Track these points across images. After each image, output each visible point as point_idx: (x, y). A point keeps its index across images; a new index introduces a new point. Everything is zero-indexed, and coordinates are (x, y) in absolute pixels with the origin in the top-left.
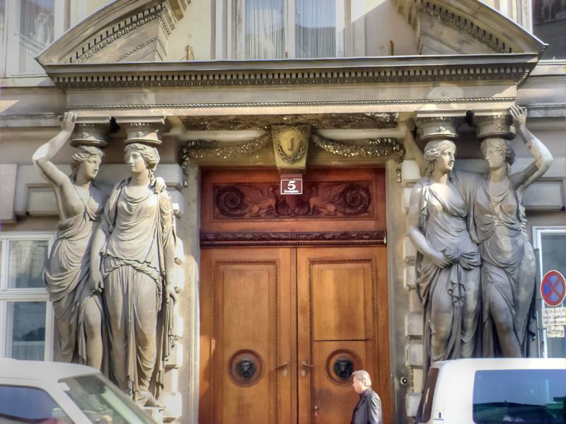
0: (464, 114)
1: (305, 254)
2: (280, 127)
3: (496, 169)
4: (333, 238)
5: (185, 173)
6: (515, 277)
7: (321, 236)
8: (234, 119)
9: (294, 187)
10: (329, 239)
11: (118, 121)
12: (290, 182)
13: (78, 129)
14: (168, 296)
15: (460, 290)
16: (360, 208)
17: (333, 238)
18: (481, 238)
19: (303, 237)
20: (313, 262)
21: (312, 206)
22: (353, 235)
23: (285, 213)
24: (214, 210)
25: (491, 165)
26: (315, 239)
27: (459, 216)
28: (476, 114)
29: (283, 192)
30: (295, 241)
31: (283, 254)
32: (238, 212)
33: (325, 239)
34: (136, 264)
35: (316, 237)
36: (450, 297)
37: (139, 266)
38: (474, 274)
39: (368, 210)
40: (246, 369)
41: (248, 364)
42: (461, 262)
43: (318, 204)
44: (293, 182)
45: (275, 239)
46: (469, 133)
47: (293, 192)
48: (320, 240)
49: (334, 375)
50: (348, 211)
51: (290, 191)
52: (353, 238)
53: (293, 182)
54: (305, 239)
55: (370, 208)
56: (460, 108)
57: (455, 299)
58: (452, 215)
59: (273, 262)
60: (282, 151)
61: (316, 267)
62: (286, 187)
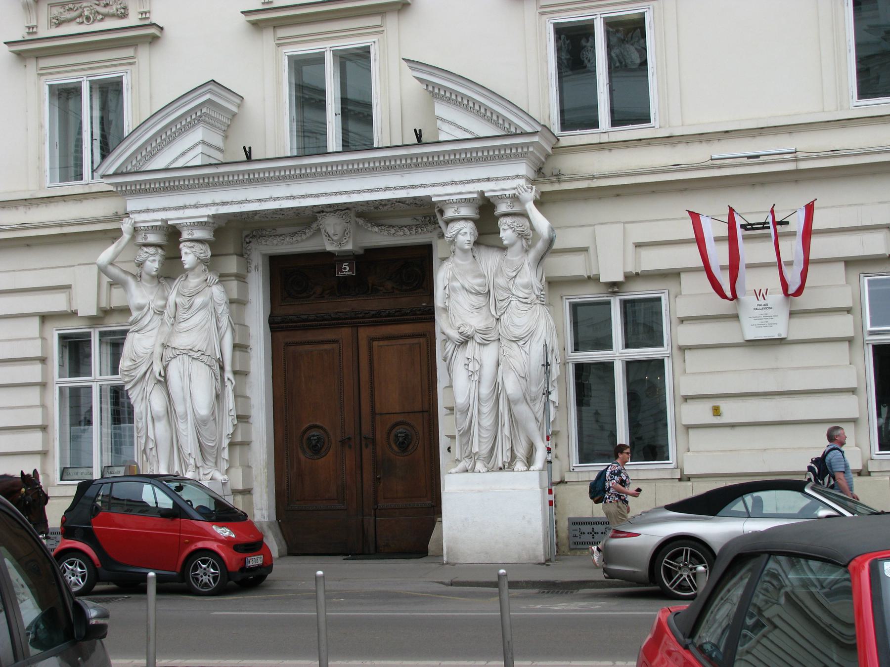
1: (364, 333)
4: (389, 315)
6: (527, 349)
7: (378, 314)
10: (386, 317)
13: (136, 230)
14: (226, 379)
17: (389, 315)
18: (499, 314)
25: (505, 242)
30: (355, 321)
31: (345, 333)
33: (381, 317)
34: (192, 353)
37: (196, 355)
38: (493, 347)
40: (314, 442)
42: (476, 337)
46: (486, 215)
48: (378, 319)
49: (394, 446)
50: (404, 288)
52: (407, 314)
54: (363, 317)
56: (472, 190)
58: (471, 293)
59: (335, 341)
61: (375, 343)
62: (340, 270)
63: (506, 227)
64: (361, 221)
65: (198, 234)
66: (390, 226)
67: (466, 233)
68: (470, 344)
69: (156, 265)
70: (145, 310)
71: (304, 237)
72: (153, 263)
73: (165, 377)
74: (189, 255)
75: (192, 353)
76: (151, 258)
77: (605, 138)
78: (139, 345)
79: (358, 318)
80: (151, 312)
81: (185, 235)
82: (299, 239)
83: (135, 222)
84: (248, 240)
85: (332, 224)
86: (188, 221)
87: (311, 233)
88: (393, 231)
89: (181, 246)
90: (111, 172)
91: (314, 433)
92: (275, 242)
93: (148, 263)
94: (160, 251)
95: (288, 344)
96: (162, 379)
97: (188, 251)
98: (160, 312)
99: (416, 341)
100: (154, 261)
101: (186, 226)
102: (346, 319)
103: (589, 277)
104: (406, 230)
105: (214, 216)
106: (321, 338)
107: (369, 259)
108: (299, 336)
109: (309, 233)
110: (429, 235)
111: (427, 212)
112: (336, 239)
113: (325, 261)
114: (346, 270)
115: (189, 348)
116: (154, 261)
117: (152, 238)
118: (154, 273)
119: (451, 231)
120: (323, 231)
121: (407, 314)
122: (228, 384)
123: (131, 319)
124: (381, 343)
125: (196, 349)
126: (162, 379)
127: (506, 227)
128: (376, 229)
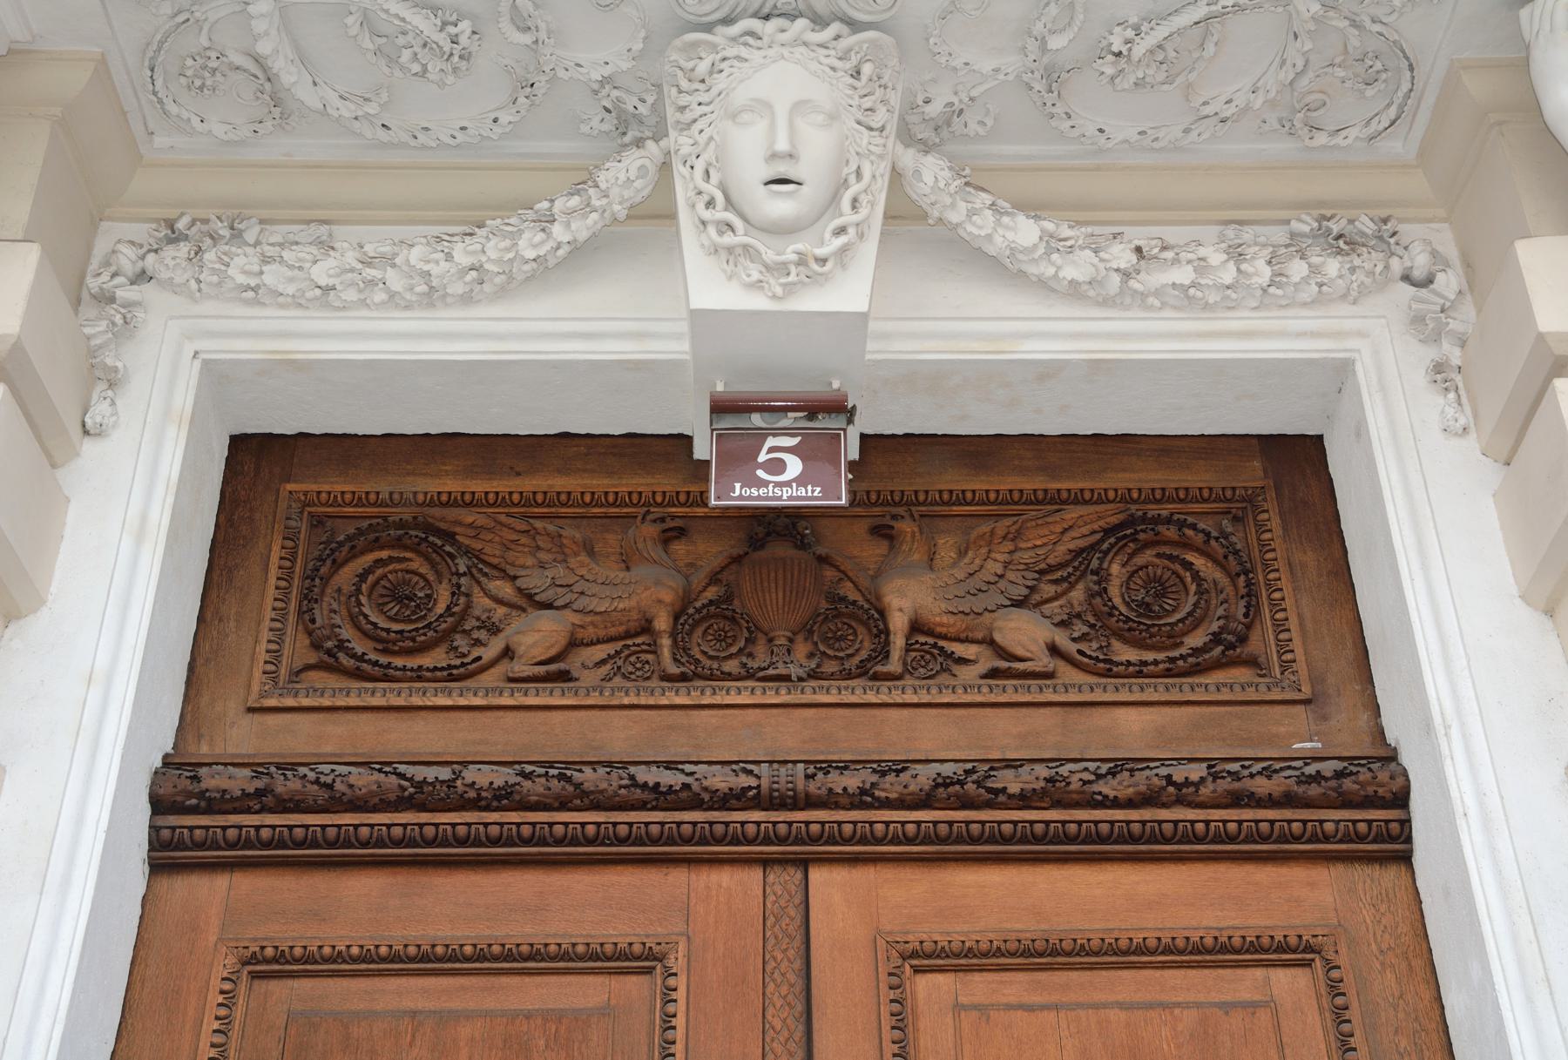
1: (852, 906)
7: (967, 787)
10: (1025, 800)
12: (771, 442)
16: (1196, 639)
17: (1052, 794)
19: (852, 781)
21: (898, 623)
22: (1179, 775)
23: (732, 666)
24: (278, 637)
26: (924, 801)
30: (785, 827)
32: (436, 658)
33: (996, 799)
35: (944, 782)
39: (1254, 645)
43: (935, 610)
45: (660, 797)
47: (786, 493)
50: (1125, 653)
54: (863, 799)
55: (1262, 641)
59: (639, 960)
60: (730, 203)
61: (931, 990)
71: (530, 244)
79: (829, 801)
82: (495, 249)
87: (582, 228)
95: (269, 965)
99: (1245, 983)
102: (727, 800)
106: (521, 931)
108: (362, 906)
110: (1342, 317)
121: (1183, 794)
124: (980, 987)
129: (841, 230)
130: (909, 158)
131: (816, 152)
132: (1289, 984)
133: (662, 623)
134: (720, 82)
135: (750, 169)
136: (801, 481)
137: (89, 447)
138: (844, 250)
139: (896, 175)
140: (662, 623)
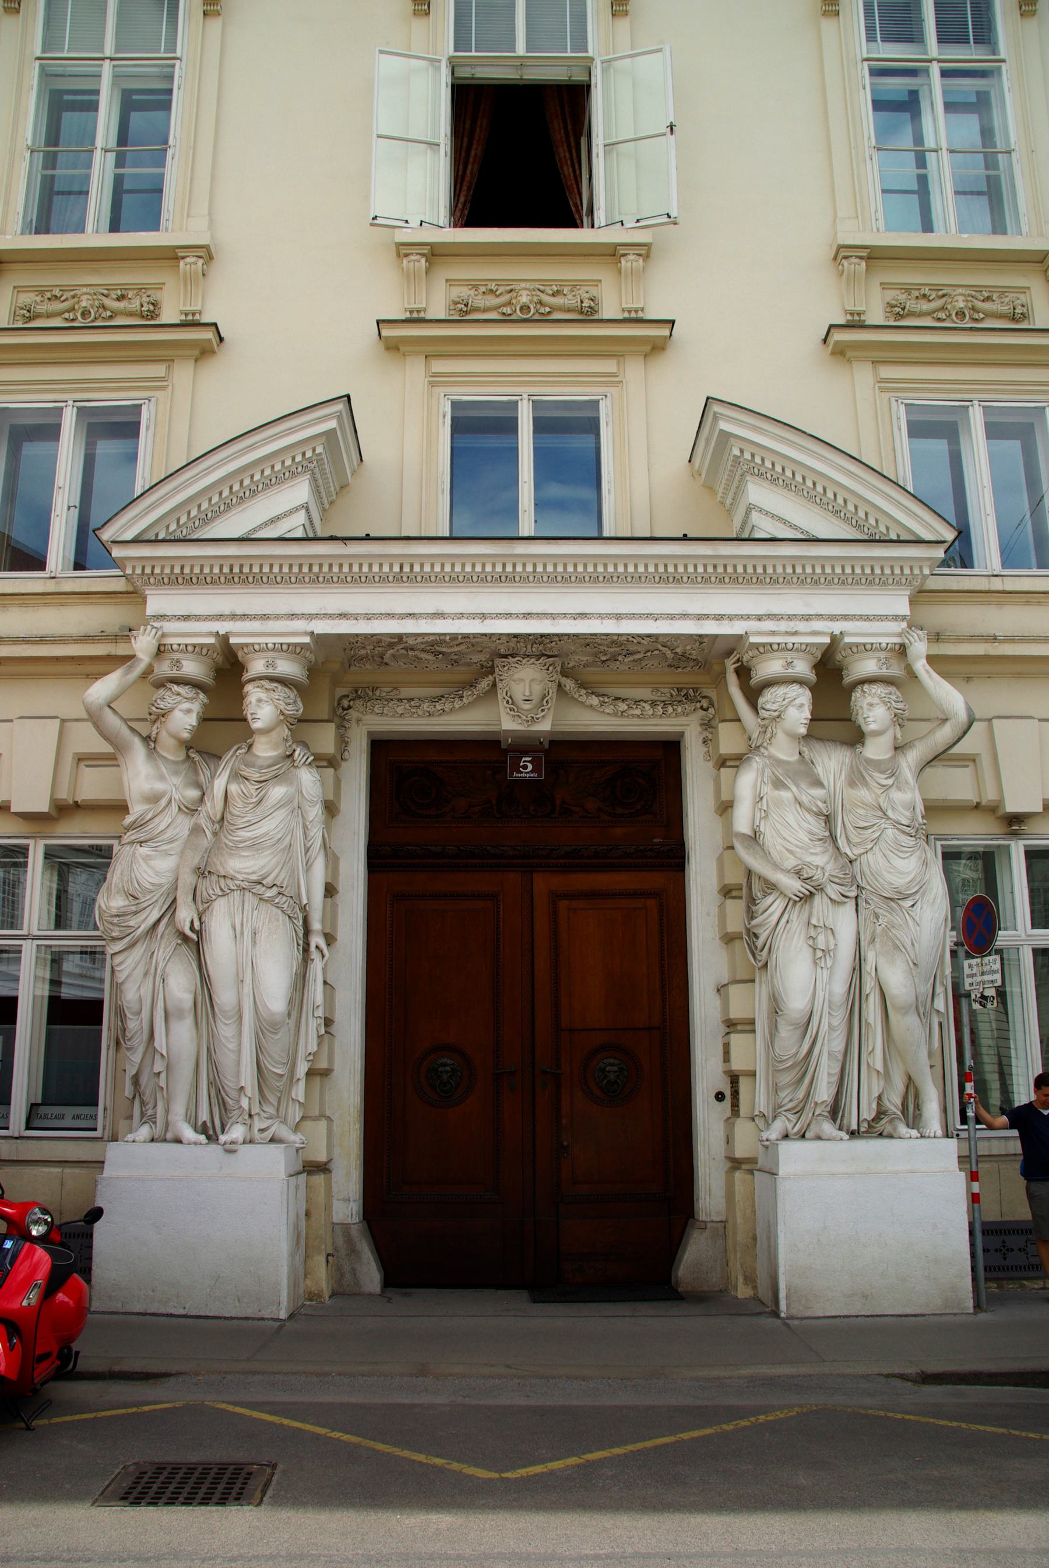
0: (827, 640)
1: (543, 883)
2: (511, 660)
3: (877, 734)
5: (343, 742)
8: (432, 644)
9: (530, 767)
11: (232, 640)
13: (161, 651)
14: (313, 948)
15: (826, 937)
20: (556, 897)
21: (558, 802)
27: (819, 814)
28: (847, 640)
29: (511, 775)
36: (811, 950)
40: (445, 1077)
41: (448, 1068)
44: (529, 759)
46: (830, 678)
51: (523, 775)
53: (529, 759)
57: (819, 954)
61: (563, 904)
62: (516, 768)
63: (876, 700)
64: (569, 684)
65: (286, 667)
66: (617, 699)
67: (801, 706)
68: (817, 899)
69: (192, 720)
70: (164, 802)
71: (457, 704)
72: (184, 715)
73: (199, 933)
74: (263, 707)
75: (260, 889)
76: (186, 706)
77: (997, 584)
78: (146, 868)
80: (174, 808)
81: (257, 666)
82: (448, 707)
83: (163, 635)
84: (345, 703)
85: (525, 680)
86: (271, 640)
87: (471, 699)
88: (623, 706)
89: (249, 688)
90: (129, 535)
91: (445, 1060)
92: (400, 710)
93: (177, 714)
94: (202, 696)
96: (194, 937)
97: (263, 695)
98: (191, 810)
100: (189, 711)
101: (264, 649)
103: (977, 806)
104: (647, 706)
105: (320, 640)
107: (564, 754)
109: (468, 696)
110: (683, 720)
111: (709, 671)
112: (521, 709)
113: (489, 752)
114: (527, 769)
115: (254, 877)
116: (189, 711)
117: (192, 668)
118: (186, 735)
119: (770, 699)
120: (501, 694)
122: (314, 954)
123: (129, 820)
125: (268, 881)
126: (194, 937)
127: (876, 700)
128: (595, 701)
129: (543, 710)
130: (564, 680)
131: (537, 689)
132: (651, 903)
133: (494, 802)
134: (511, 672)
135: (519, 697)
136: (532, 772)
137: (343, 764)
138: (543, 717)
139: (559, 685)
140: (494, 802)
